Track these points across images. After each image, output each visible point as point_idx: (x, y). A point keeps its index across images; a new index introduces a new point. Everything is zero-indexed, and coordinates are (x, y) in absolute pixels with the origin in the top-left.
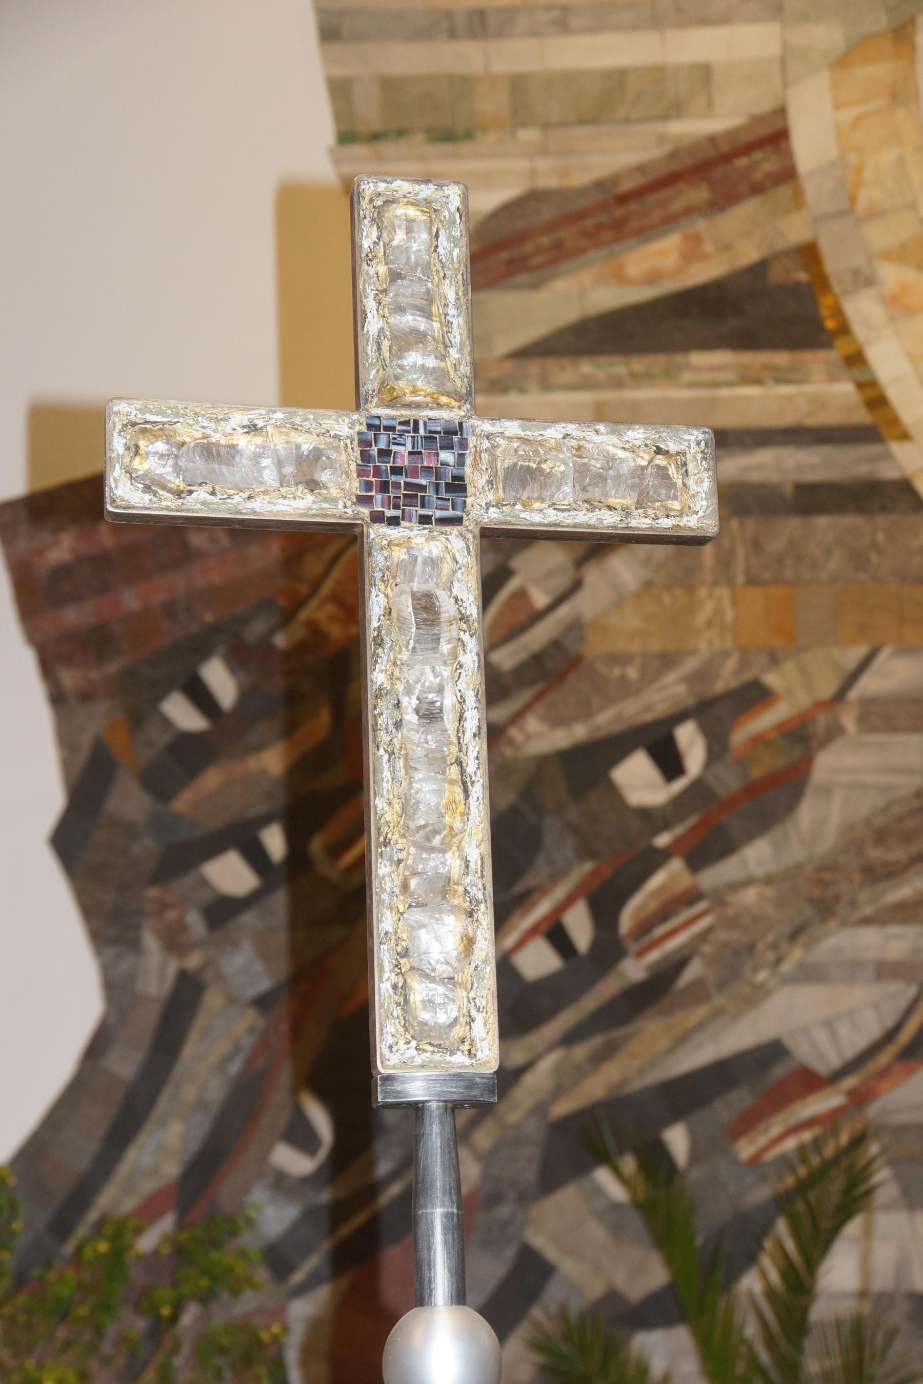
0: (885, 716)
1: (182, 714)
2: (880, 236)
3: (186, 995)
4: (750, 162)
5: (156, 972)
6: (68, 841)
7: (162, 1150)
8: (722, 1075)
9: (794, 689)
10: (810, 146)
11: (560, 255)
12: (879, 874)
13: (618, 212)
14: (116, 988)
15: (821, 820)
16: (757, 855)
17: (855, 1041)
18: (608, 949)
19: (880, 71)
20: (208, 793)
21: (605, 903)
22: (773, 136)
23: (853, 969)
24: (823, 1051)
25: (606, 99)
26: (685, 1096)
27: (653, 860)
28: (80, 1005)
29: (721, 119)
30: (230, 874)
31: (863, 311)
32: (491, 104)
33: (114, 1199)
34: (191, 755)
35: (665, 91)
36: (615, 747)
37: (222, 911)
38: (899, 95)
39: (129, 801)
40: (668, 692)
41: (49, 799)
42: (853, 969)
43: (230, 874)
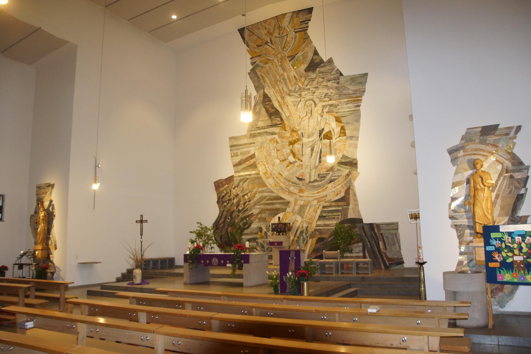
0: (259, 192)
1: (223, 194)
2: (260, 160)
3: (223, 211)
4: (253, 156)
5: (222, 210)
6: (218, 202)
7: (222, 220)
8: (250, 215)
9: (255, 190)
10: (256, 155)
11: (243, 163)
12: (258, 202)
13: (246, 160)
14: (220, 211)
15: (256, 199)
16: (252, 202)
17: (257, 212)
18: (244, 208)
19: (260, 150)
20: (224, 199)
21: (244, 204)
22: (254, 154)
23: (257, 208)
24: (255, 213)
25: (245, 153)
26: (248, 216)
27: (246, 202)
28: (218, 212)
29: (252, 153)
30: (225, 204)
31: (259, 165)
32: (239, 154)
33: (220, 223)
34: (224, 197)
35: (249, 152)
36: (245, 195)
37: (225, 206)
38: (261, 151)
39: (220, 200)
40: (248, 191)
41: (217, 200)
42: (257, 208)
43: (225, 204)
